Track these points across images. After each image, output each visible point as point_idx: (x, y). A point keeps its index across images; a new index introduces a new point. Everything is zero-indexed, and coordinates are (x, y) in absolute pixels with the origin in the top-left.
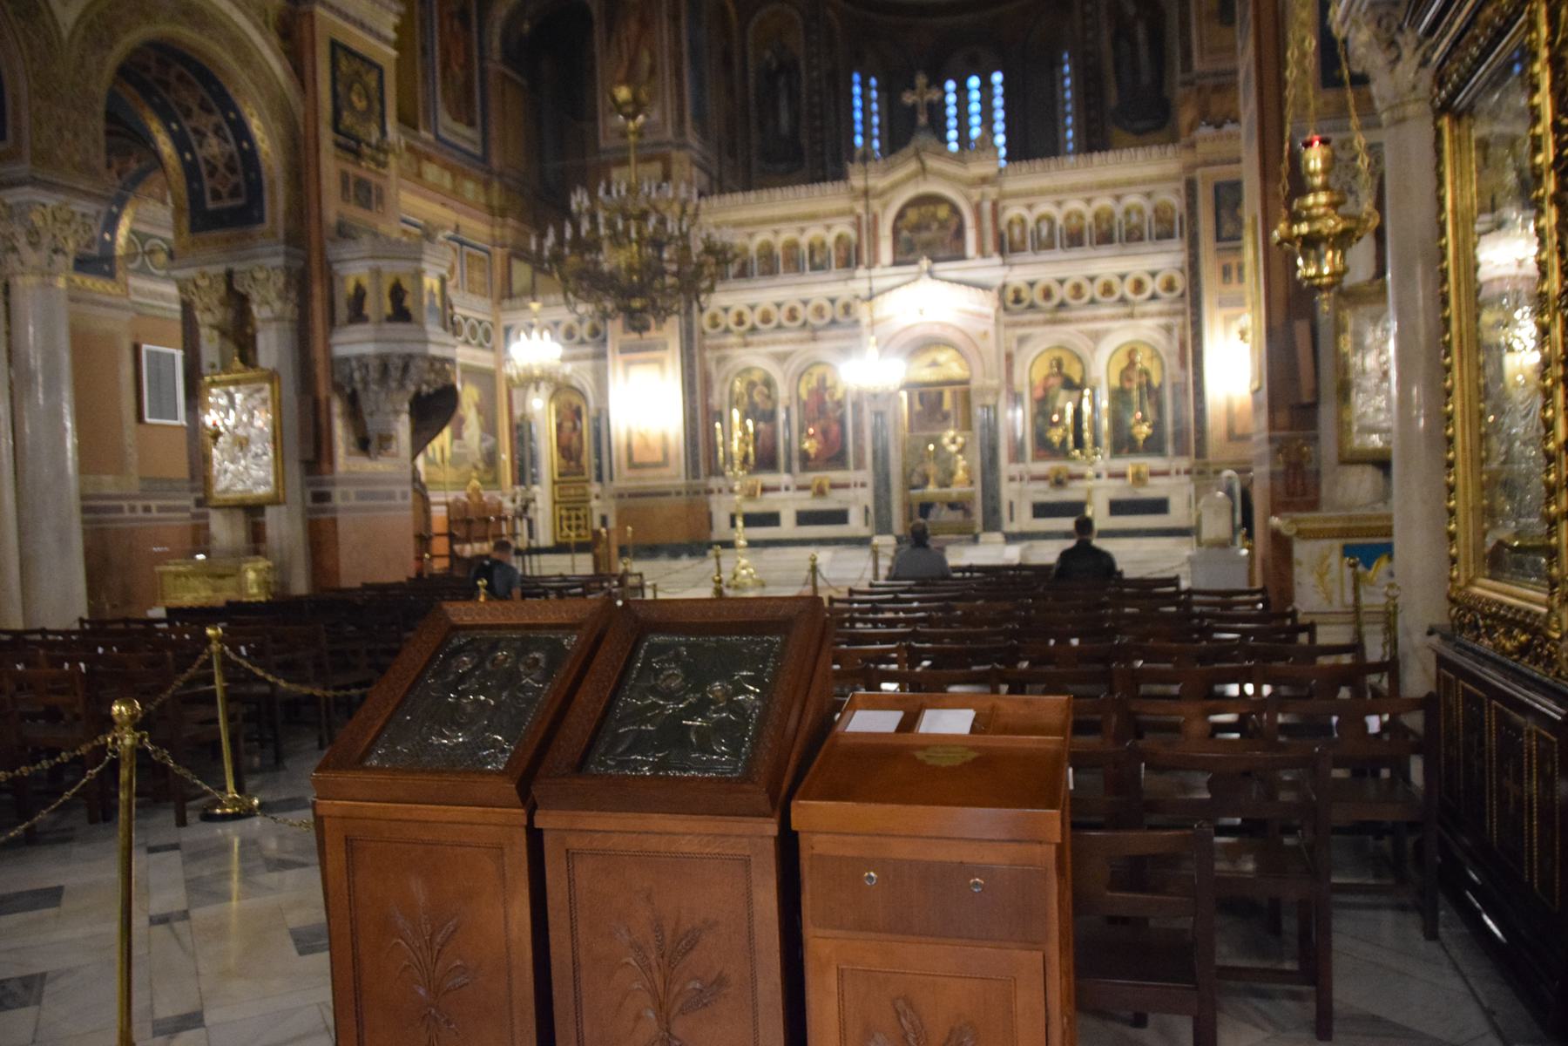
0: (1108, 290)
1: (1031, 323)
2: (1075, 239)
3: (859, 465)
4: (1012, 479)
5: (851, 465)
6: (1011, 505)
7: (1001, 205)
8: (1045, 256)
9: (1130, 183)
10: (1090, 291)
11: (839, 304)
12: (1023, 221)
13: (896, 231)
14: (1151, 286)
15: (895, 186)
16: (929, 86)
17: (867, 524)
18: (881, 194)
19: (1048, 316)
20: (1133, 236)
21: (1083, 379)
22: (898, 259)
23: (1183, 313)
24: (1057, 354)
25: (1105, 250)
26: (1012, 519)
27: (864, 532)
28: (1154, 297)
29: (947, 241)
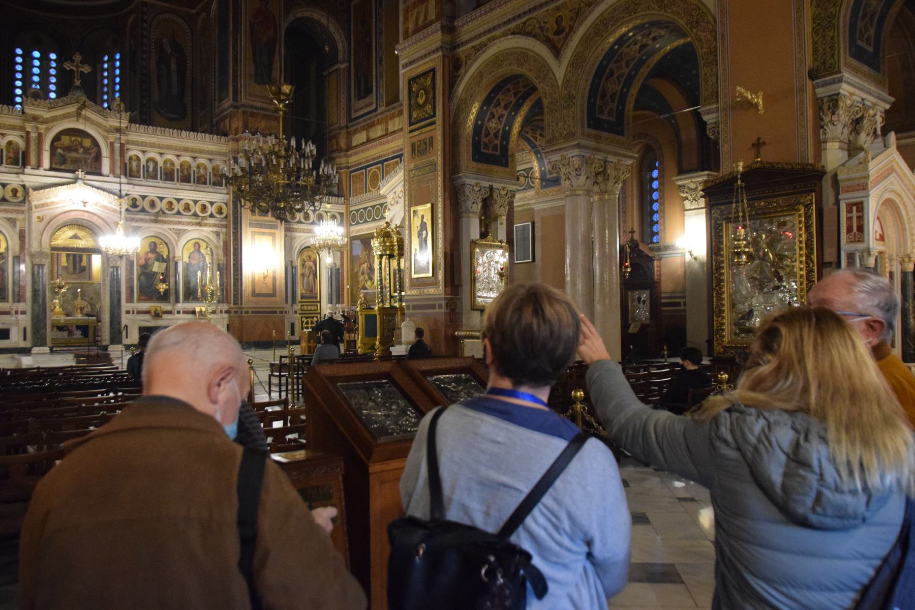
0: (187, 208)
1: (142, 220)
2: (169, 176)
3: (19, 298)
4: (128, 312)
7: (127, 146)
8: (151, 182)
9: (201, 151)
10: (177, 207)
11: (9, 188)
12: (138, 159)
13: (53, 149)
14: (211, 209)
15: (54, 119)
16: (82, 62)
17: (25, 339)
18: (45, 121)
19: (153, 218)
20: (201, 181)
21: (168, 256)
22: (54, 166)
23: (226, 226)
24: (153, 240)
25: (186, 186)
26: (127, 337)
27: (22, 344)
28: (212, 216)
29: (89, 161)
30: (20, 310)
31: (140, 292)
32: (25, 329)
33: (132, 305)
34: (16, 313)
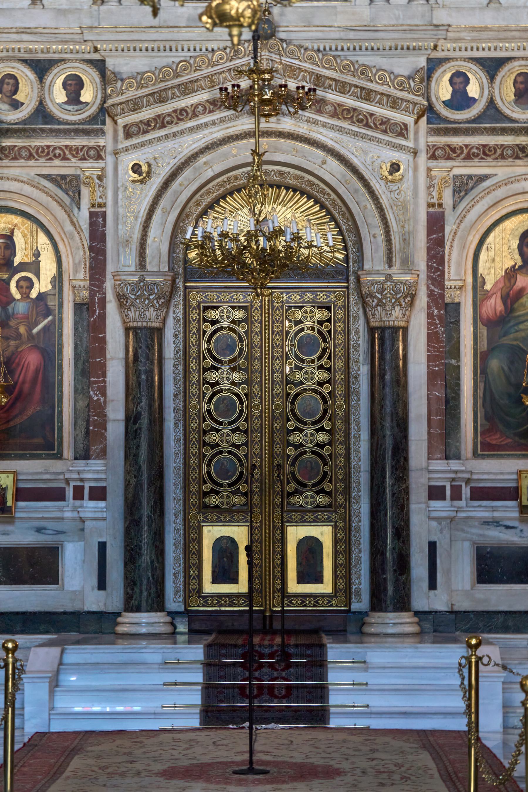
5: (68, 452)
6: (432, 546)
17: (102, 585)
26: (433, 585)
30: (87, 485)
31: (487, 418)
32: (102, 546)
33: (454, 465)
34: (78, 493)
